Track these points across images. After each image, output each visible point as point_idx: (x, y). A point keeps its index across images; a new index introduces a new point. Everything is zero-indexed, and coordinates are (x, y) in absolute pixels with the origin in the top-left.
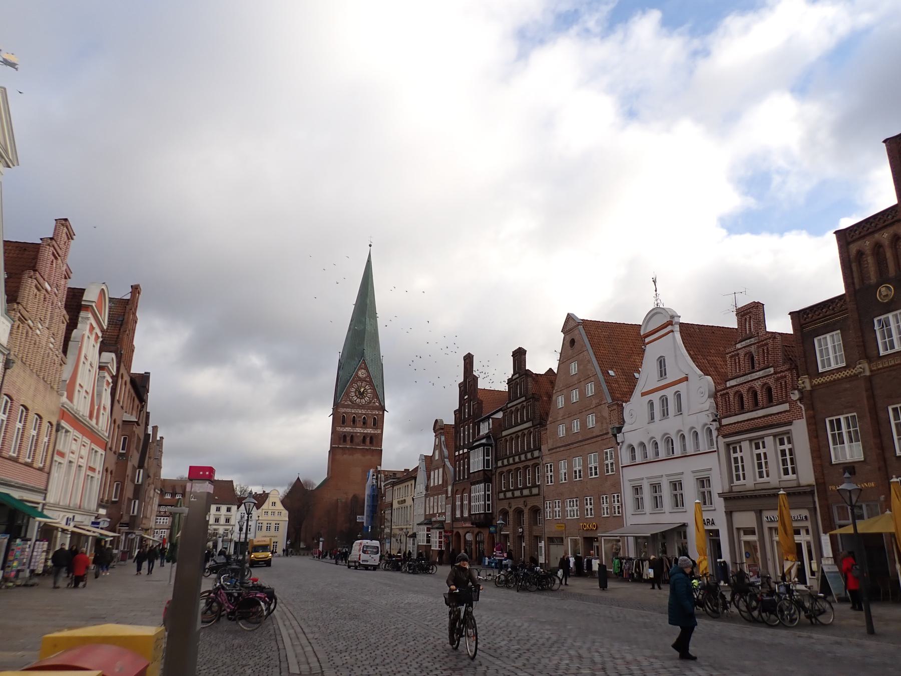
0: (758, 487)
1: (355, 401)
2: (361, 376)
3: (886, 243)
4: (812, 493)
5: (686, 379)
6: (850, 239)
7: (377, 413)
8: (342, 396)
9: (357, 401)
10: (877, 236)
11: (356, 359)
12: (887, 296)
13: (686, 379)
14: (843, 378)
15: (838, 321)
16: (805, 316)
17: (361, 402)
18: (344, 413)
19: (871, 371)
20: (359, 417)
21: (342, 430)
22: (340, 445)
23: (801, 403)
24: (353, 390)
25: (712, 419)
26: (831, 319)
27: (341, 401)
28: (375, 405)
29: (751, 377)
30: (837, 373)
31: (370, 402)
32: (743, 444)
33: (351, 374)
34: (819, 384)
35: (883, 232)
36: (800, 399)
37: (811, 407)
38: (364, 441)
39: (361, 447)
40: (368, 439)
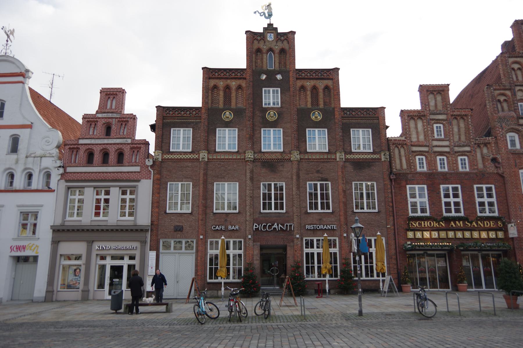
0: (94, 224)
3: (234, 88)
4: (147, 231)
5: (30, 126)
6: (211, 76)
10: (229, 81)
12: (228, 117)
13: (30, 126)
14: (187, 159)
15: (193, 123)
16: (168, 112)
19: (208, 159)
23: (151, 168)
25: (59, 165)
26: (186, 119)
29: (126, 141)
30: (184, 155)
32: (86, 189)
34: (168, 159)
35: (233, 80)
36: (152, 166)
37: (160, 173)
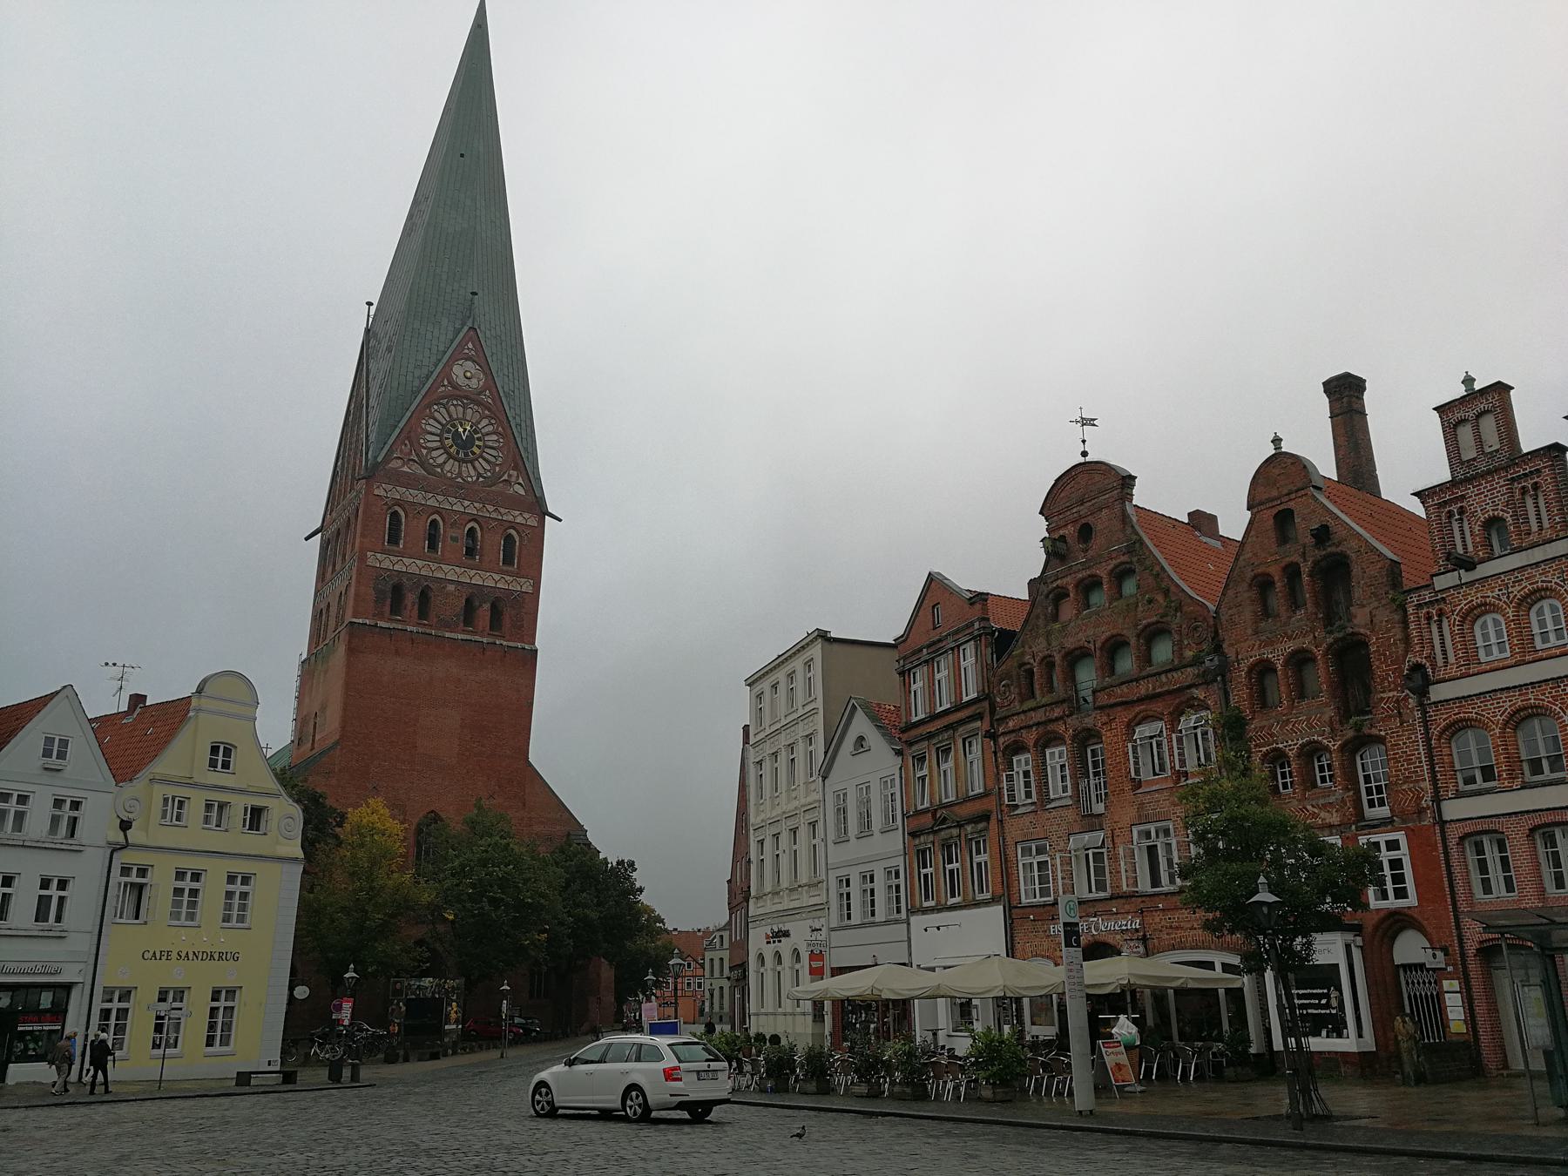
1: (441, 466)
2: (461, 381)
7: (519, 520)
8: (390, 442)
9: (447, 467)
11: (445, 321)
17: (460, 474)
18: (398, 503)
20: (453, 525)
21: (386, 564)
22: (381, 616)
24: (433, 428)
27: (387, 459)
28: (511, 491)
31: (495, 480)
33: (425, 371)
38: (469, 613)
39: (460, 636)
40: (487, 606)
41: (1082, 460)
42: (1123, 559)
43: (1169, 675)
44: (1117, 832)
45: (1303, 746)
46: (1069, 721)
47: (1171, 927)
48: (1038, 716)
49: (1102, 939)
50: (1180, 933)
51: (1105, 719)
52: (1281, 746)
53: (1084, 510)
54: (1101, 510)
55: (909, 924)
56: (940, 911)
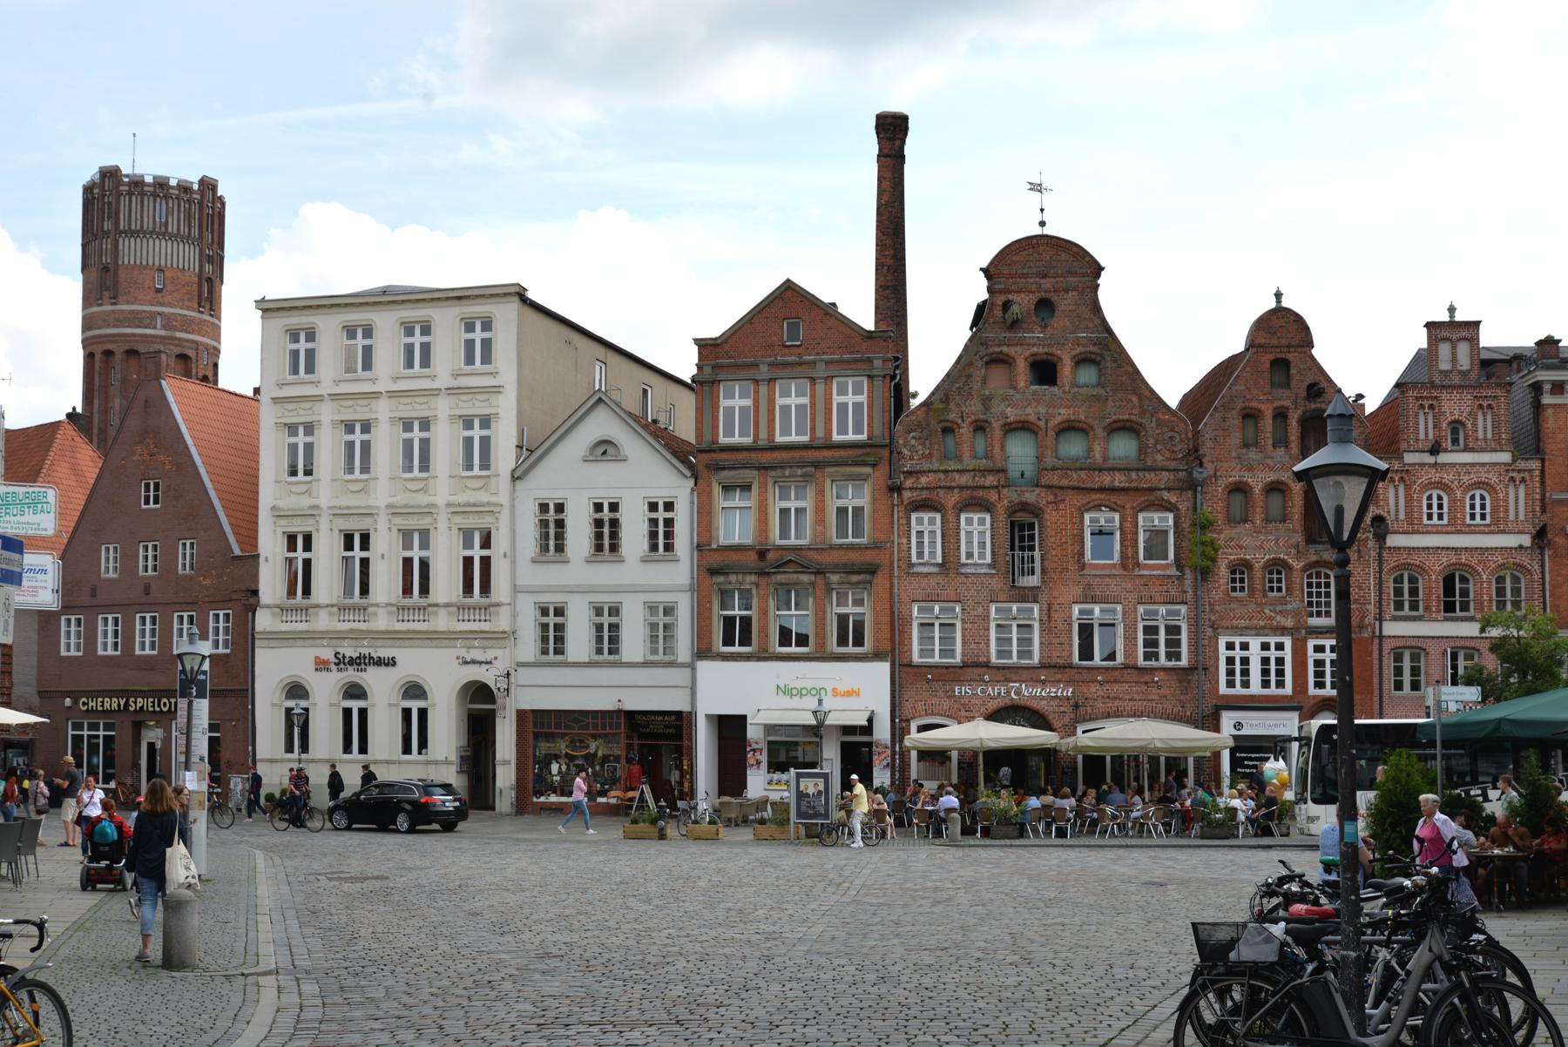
41: (1038, 231)
42: (1092, 348)
43: (1141, 474)
44: (1056, 607)
45: (1269, 560)
46: (1005, 491)
47: (1108, 697)
48: (964, 480)
49: (1022, 703)
50: (1117, 703)
51: (1051, 498)
52: (1248, 557)
53: (1047, 284)
54: (1067, 291)
55: (694, 669)
56: (759, 659)
